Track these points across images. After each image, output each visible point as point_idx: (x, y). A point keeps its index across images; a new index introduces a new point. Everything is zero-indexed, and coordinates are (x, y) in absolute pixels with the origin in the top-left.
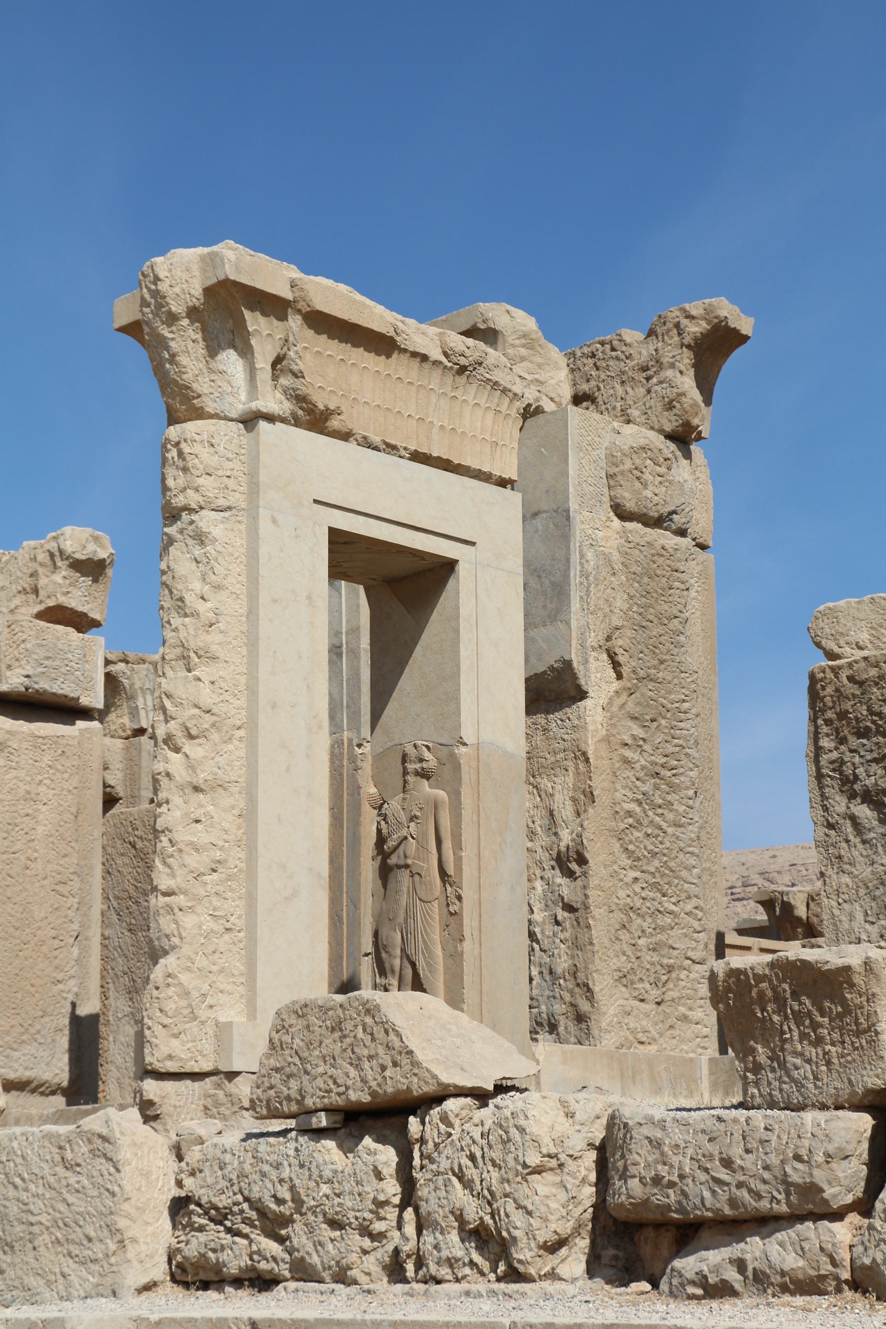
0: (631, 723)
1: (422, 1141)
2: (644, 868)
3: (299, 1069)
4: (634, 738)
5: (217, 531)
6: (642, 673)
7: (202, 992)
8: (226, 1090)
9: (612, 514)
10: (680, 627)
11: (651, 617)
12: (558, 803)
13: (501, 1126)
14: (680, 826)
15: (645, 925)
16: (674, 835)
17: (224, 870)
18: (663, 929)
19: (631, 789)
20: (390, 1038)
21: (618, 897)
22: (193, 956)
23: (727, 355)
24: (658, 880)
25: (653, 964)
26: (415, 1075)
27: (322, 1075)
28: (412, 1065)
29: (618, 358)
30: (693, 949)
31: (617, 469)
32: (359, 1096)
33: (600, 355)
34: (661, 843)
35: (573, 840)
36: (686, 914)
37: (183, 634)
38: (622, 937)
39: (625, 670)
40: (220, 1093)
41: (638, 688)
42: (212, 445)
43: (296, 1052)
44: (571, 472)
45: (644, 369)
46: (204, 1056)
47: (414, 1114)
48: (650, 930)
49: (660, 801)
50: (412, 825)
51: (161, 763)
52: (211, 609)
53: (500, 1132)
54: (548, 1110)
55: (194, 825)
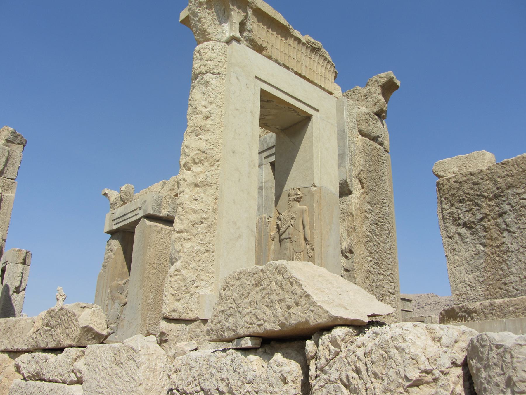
0: (367, 204)
1: (316, 357)
2: (373, 257)
3: (235, 311)
4: (369, 209)
5: (213, 82)
6: (371, 188)
7: (192, 279)
8: (201, 328)
9: (359, 134)
10: (382, 174)
11: (373, 169)
12: (341, 232)
13: (382, 347)
14: (384, 243)
15: (374, 278)
16: (383, 246)
17: (207, 223)
18: (380, 280)
19: (368, 228)
20: (293, 288)
21: (365, 266)
22: (189, 261)
23: (392, 93)
24: (378, 262)
25: (377, 293)
26: (312, 311)
27: (248, 314)
28: (310, 305)
29: (356, 94)
30: (391, 289)
31: (360, 119)
32: (272, 326)
33: (349, 95)
34: (379, 248)
35: (348, 245)
36: (388, 275)
37: (195, 122)
38: (367, 282)
39: (365, 186)
40: (198, 330)
41: (369, 192)
42: (213, 50)
43: (234, 301)
44: (345, 117)
45: (365, 95)
46: (192, 311)
47: (310, 338)
48: (376, 280)
49: (378, 233)
50: (292, 221)
51: (182, 176)
52: (208, 111)
53: (382, 352)
54: (419, 336)
55: (194, 201)
